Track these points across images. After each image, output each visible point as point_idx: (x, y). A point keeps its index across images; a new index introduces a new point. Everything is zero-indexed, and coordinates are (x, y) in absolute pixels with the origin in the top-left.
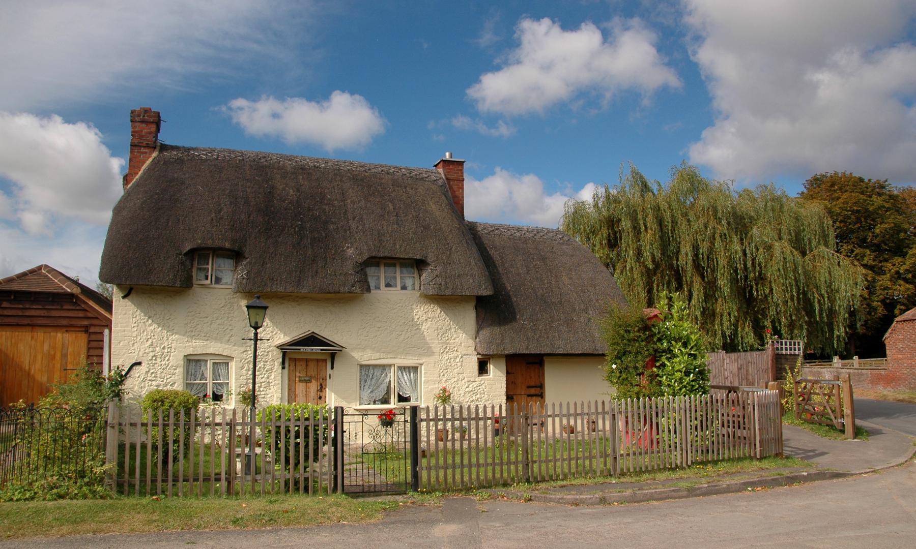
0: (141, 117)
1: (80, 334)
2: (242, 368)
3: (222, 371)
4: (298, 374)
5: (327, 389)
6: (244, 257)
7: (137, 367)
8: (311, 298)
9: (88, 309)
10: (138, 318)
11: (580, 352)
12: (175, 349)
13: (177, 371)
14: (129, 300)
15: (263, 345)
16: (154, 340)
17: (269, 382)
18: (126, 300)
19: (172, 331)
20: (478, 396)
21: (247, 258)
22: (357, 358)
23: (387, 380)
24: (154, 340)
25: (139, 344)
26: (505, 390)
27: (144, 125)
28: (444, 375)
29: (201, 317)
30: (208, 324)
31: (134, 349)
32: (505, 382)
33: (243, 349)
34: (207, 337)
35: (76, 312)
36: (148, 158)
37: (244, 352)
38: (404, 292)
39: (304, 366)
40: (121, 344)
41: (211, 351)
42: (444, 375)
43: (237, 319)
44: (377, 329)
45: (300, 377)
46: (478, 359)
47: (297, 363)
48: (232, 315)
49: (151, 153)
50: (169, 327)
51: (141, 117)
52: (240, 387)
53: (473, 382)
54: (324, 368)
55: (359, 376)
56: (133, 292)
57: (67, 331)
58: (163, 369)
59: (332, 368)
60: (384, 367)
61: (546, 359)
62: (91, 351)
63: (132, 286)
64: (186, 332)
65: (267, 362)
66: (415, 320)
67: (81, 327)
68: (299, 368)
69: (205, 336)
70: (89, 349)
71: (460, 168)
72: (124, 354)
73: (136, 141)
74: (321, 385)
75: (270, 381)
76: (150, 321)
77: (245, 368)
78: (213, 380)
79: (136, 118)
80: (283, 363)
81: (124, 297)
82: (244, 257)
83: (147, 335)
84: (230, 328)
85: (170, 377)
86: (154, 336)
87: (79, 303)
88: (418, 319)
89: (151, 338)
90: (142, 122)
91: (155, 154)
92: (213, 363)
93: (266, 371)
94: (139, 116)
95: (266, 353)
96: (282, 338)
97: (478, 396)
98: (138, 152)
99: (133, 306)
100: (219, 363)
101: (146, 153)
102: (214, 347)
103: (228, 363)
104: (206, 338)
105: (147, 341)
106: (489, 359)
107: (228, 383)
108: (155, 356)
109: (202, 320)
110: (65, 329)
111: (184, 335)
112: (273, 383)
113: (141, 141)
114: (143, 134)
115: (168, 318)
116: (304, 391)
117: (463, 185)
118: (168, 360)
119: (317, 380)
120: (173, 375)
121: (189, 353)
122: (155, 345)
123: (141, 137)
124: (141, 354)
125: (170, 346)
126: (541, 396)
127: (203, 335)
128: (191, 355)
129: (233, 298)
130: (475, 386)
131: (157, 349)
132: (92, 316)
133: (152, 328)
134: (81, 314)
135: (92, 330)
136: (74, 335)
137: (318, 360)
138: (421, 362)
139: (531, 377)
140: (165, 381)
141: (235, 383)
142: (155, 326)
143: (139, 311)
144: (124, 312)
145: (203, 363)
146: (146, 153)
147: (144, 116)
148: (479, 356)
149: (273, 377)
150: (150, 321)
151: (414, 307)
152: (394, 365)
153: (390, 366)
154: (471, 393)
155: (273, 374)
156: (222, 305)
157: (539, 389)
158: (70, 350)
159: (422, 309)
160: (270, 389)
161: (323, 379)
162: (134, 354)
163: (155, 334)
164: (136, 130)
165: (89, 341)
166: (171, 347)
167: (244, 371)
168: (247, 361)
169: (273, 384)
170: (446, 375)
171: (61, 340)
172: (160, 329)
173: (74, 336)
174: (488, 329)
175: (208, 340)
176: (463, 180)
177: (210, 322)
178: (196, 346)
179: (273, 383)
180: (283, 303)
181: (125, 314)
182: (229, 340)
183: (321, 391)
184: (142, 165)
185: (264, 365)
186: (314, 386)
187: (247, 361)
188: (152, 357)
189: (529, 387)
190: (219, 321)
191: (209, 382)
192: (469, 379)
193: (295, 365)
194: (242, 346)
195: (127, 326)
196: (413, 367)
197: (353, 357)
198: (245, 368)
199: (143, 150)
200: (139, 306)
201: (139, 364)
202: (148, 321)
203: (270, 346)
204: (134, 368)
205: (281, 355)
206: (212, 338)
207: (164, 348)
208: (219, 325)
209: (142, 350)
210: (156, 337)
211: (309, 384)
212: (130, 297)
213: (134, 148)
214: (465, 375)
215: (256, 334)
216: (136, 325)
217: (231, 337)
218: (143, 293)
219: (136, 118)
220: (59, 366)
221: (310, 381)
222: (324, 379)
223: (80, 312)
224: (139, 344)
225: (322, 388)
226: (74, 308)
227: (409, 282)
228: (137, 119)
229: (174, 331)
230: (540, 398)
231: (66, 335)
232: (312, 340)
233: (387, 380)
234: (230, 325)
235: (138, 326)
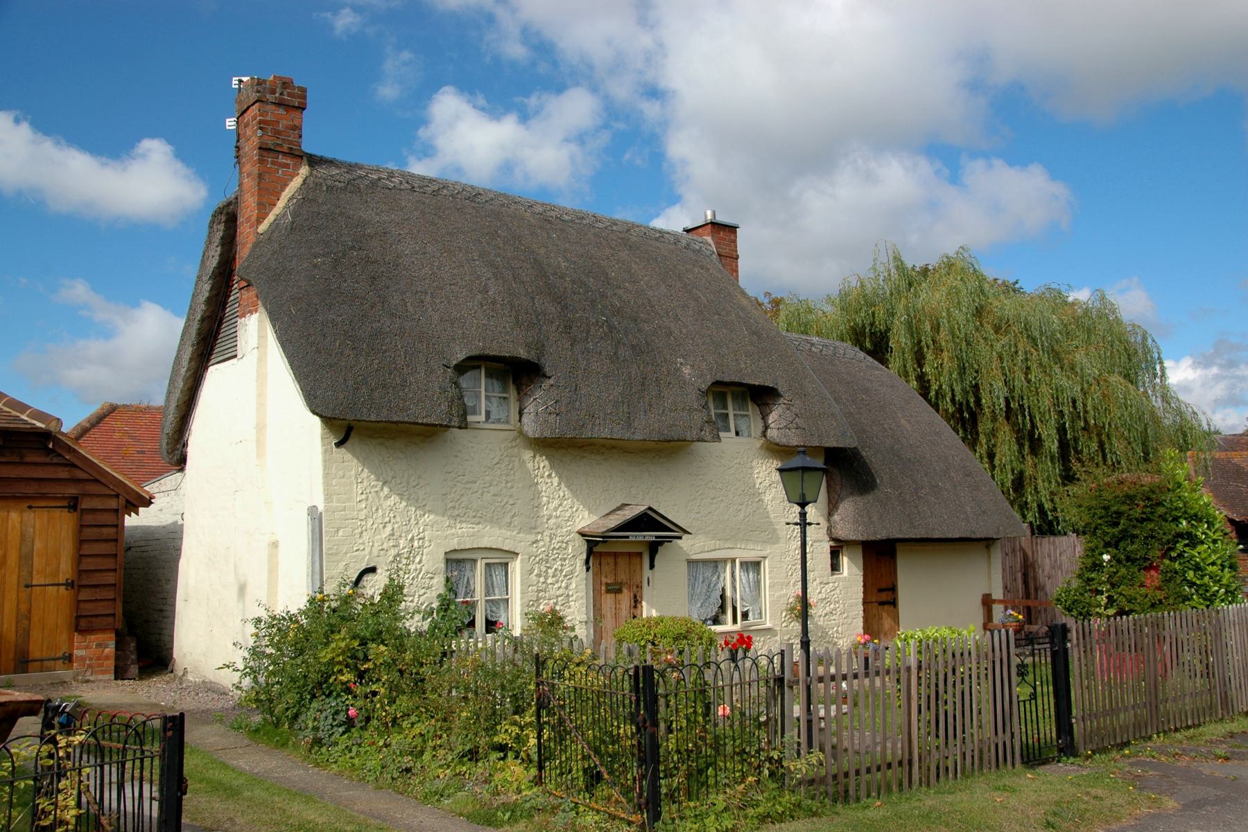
0: (277, 95)
1: (57, 513)
2: (531, 572)
3: (498, 577)
4: (604, 580)
5: (644, 604)
6: (545, 376)
7: (368, 578)
8: (621, 449)
9: (78, 463)
10: (365, 484)
11: (958, 536)
12: (430, 541)
13: (435, 581)
14: (346, 449)
15: (559, 531)
16: (396, 526)
17: (568, 595)
18: (343, 450)
19: (422, 507)
20: (832, 606)
21: (549, 378)
22: (685, 549)
23: (720, 586)
24: (396, 526)
25: (370, 533)
26: (862, 595)
27: (281, 111)
28: (792, 575)
29: (467, 483)
30: (478, 495)
31: (363, 544)
32: (862, 584)
33: (532, 538)
34: (479, 519)
35: (52, 469)
36: (293, 176)
37: (533, 543)
38: (739, 439)
39: (612, 565)
40: (341, 533)
41: (485, 543)
42: (792, 575)
43: (520, 485)
44: (711, 501)
45: (607, 584)
46: (831, 547)
47: (603, 561)
48: (512, 477)
49: (296, 168)
50: (417, 501)
51: (277, 95)
52: (528, 606)
53: (826, 584)
54: (638, 566)
55: (686, 579)
56: (353, 434)
57: (30, 507)
58: (413, 579)
59: (652, 566)
60: (716, 564)
61: (899, 547)
62: (85, 546)
63: (353, 424)
64: (446, 510)
65: (565, 559)
66: (757, 486)
67: (64, 498)
68: (605, 568)
69: (474, 517)
70: (81, 542)
71: (732, 237)
72: (346, 553)
73: (270, 142)
74: (635, 597)
75: (570, 593)
76: (386, 490)
77: (536, 572)
78: (486, 596)
79: (268, 96)
80: (587, 562)
81: (339, 445)
82: (545, 376)
83: (383, 516)
84: (511, 502)
85: (424, 593)
86: (394, 517)
87: (59, 451)
88: (760, 483)
89: (390, 522)
90: (279, 104)
91: (304, 170)
92: (486, 564)
93: (565, 576)
94: (273, 92)
95: (564, 545)
96: (586, 519)
97: (832, 606)
98: (273, 163)
99: (355, 461)
100: (494, 564)
101: (287, 166)
102: (491, 536)
103: (507, 564)
104: (477, 520)
105: (384, 527)
106: (842, 547)
107: (507, 600)
108: (398, 555)
109: (468, 486)
110: (25, 505)
111: (443, 516)
112: (574, 597)
113: (279, 142)
114: (281, 127)
115: (415, 483)
116: (613, 609)
117: (737, 266)
118: (420, 562)
119: (629, 588)
120: (428, 588)
121: (452, 549)
122: (397, 534)
123: (277, 133)
124: (375, 552)
125: (421, 535)
126: (894, 603)
127: (472, 514)
128: (455, 551)
129: (512, 447)
130: (829, 591)
131: (401, 542)
132: (85, 476)
133: (391, 502)
134: (63, 473)
135: (86, 504)
136: (45, 514)
137: (630, 555)
138: (764, 553)
139: (882, 575)
140: (416, 600)
141: (522, 598)
142: (394, 499)
143: (366, 470)
144: (341, 473)
145: (468, 566)
146: (287, 166)
147: (282, 94)
148: (832, 543)
149: (573, 586)
150: (386, 490)
151: (754, 464)
152: (733, 561)
153: (725, 561)
154: (825, 602)
155: (574, 580)
156: (496, 461)
157: (891, 592)
158: (38, 545)
159: (764, 467)
160: (570, 608)
161: (637, 587)
162: (363, 553)
163: (397, 514)
164: (268, 118)
165: (82, 527)
166: (423, 538)
167: (533, 577)
168: (537, 559)
169: (574, 598)
170: (794, 574)
171: (18, 525)
172: (404, 504)
173: (45, 518)
174: (851, 499)
175: (478, 524)
176: (737, 258)
177: (480, 492)
178: (463, 535)
179: (574, 597)
180: (584, 457)
181: (343, 477)
182: (511, 523)
183: (635, 607)
184: (283, 189)
185: (562, 565)
186: (625, 598)
187: (537, 559)
188: (395, 556)
189: (880, 590)
190: (493, 490)
191: (479, 595)
192: (821, 580)
193: (600, 564)
194: (531, 533)
195: (349, 500)
196: (751, 562)
197: (681, 548)
198: (536, 572)
199: (281, 159)
200: (365, 461)
201: (372, 570)
202: (382, 489)
203: (569, 533)
204: (365, 578)
205: (585, 548)
206: (485, 520)
207: (412, 540)
208: (494, 495)
209: (376, 544)
210: (398, 519)
211: (619, 596)
212: (348, 444)
213: (265, 153)
214: (816, 573)
215: (803, 515)
216: (364, 497)
217: (513, 516)
218: (371, 437)
219: (268, 96)
220: (15, 577)
221: (619, 591)
222: (639, 587)
223: (61, 469)
224: (370, 533)
225: (636, 602)
226: (47, 460)
227: (743, 427)
228: (270, 97)
229: (427, 508)
230: (892, 608)
231: (29, 516)
232: (646, 521)
233: (720, 586)
234: (511, 496)
235: (367, 500)
